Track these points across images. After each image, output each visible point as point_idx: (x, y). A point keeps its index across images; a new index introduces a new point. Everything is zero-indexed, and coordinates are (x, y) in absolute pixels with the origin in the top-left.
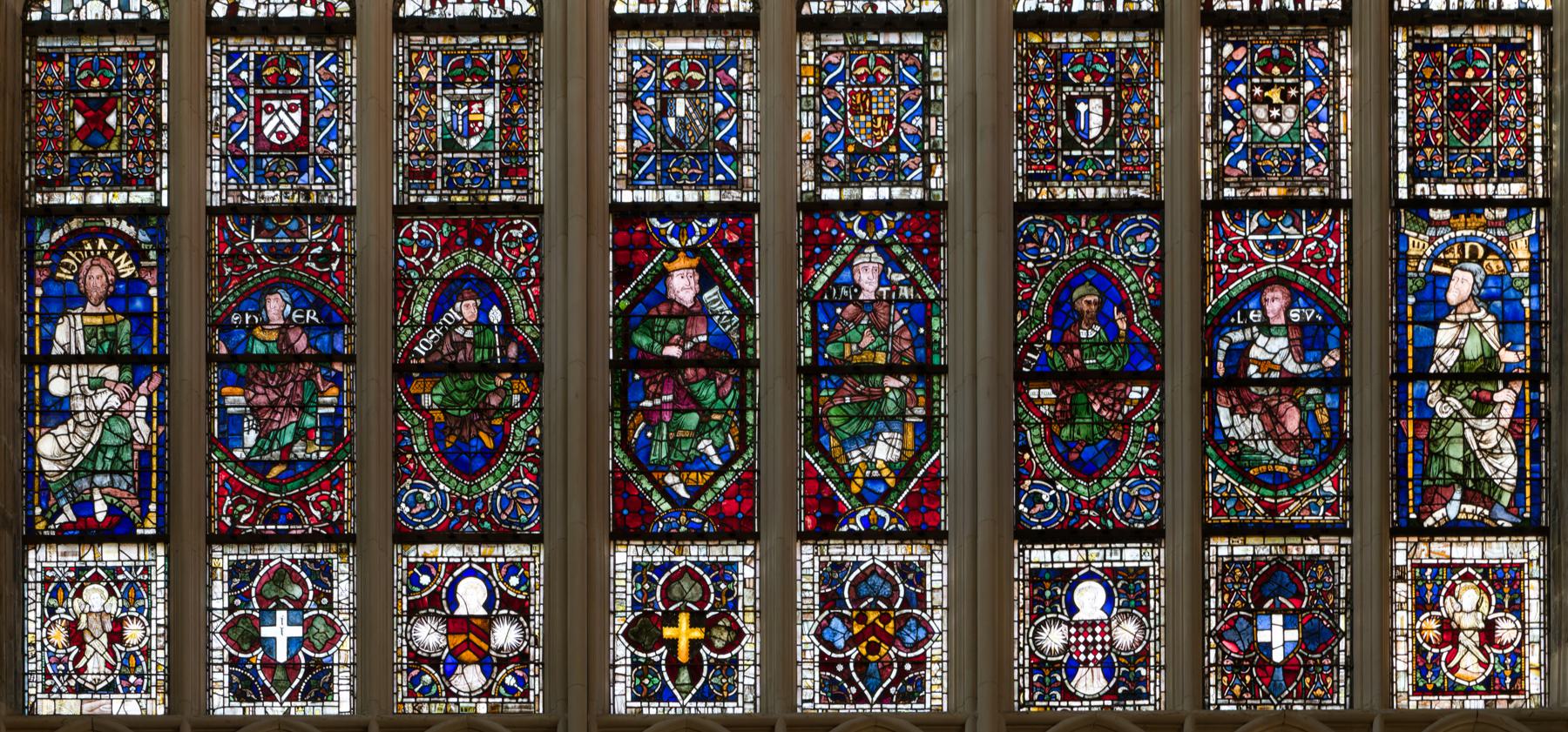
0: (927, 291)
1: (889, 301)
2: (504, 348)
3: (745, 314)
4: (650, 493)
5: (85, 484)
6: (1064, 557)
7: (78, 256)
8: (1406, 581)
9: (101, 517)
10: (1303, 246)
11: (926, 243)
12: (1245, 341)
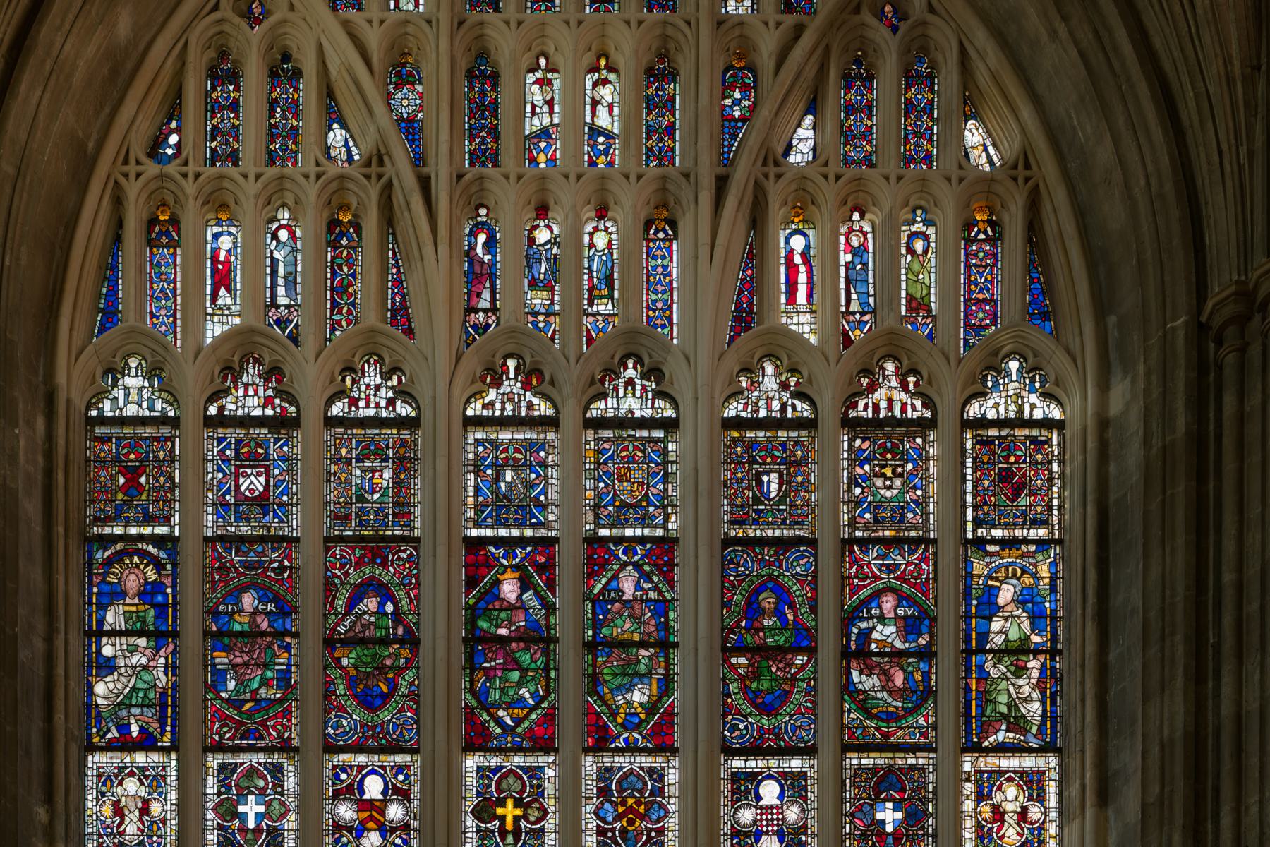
0: (666, 594)
1: (642, 601)
2: (395, 628)
3: (549, 608)
4: (488, 722)
5: (124, 713)
6: (753, 764)
8: (971, 781)
9: (135, 735)
10: (906, 568)
11: (666, 564)
12: (868, 628)
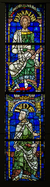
7: (20, 15)
9: (26, 87)
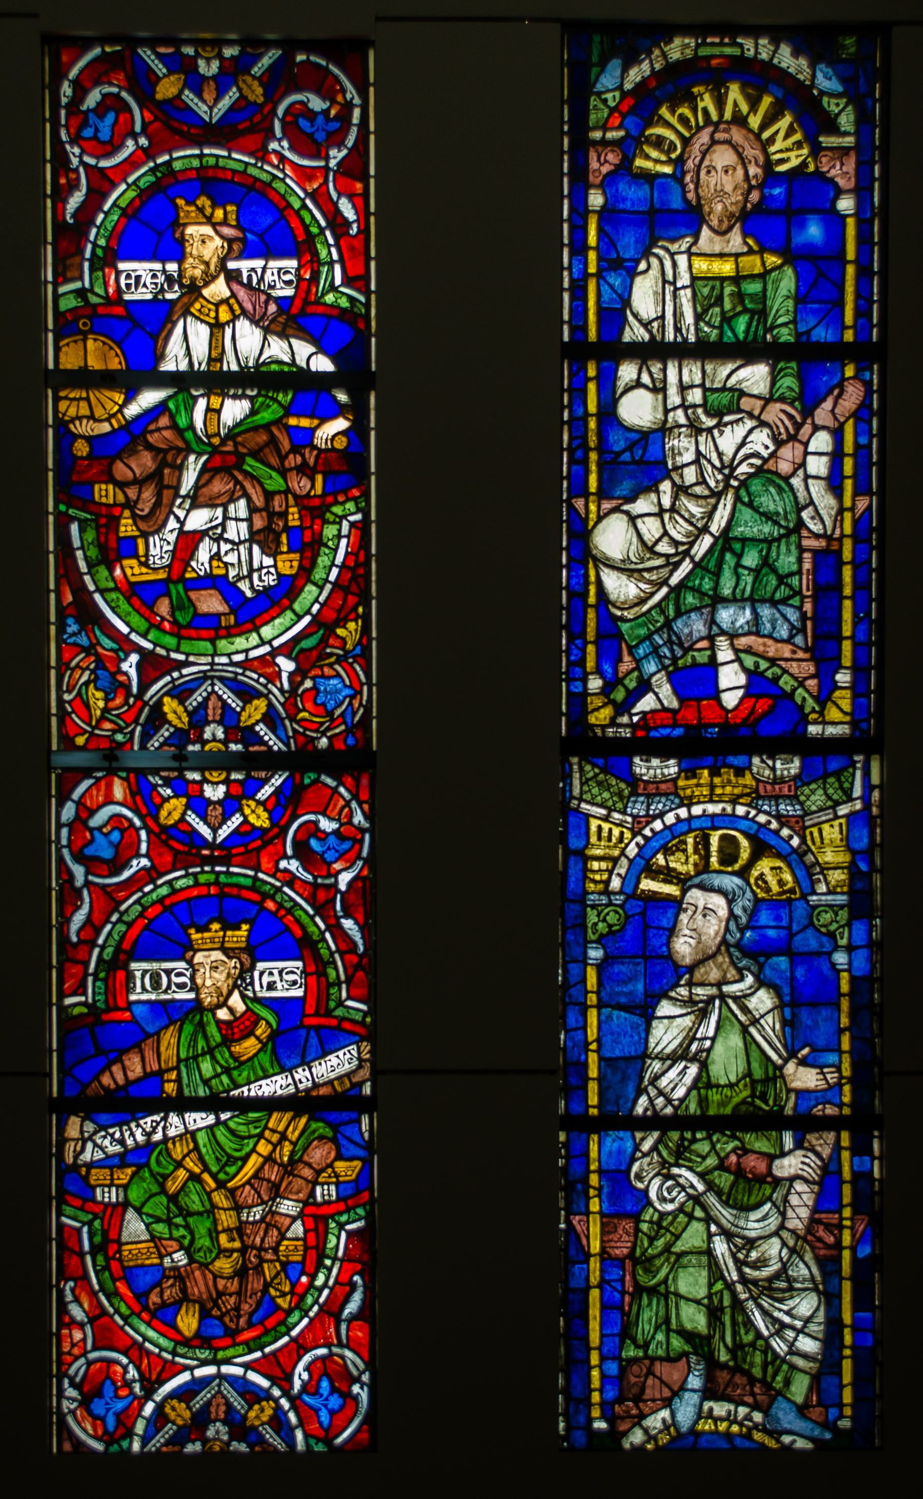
5: (698, 626)
7: (683, 120)
9: (730, 700)
